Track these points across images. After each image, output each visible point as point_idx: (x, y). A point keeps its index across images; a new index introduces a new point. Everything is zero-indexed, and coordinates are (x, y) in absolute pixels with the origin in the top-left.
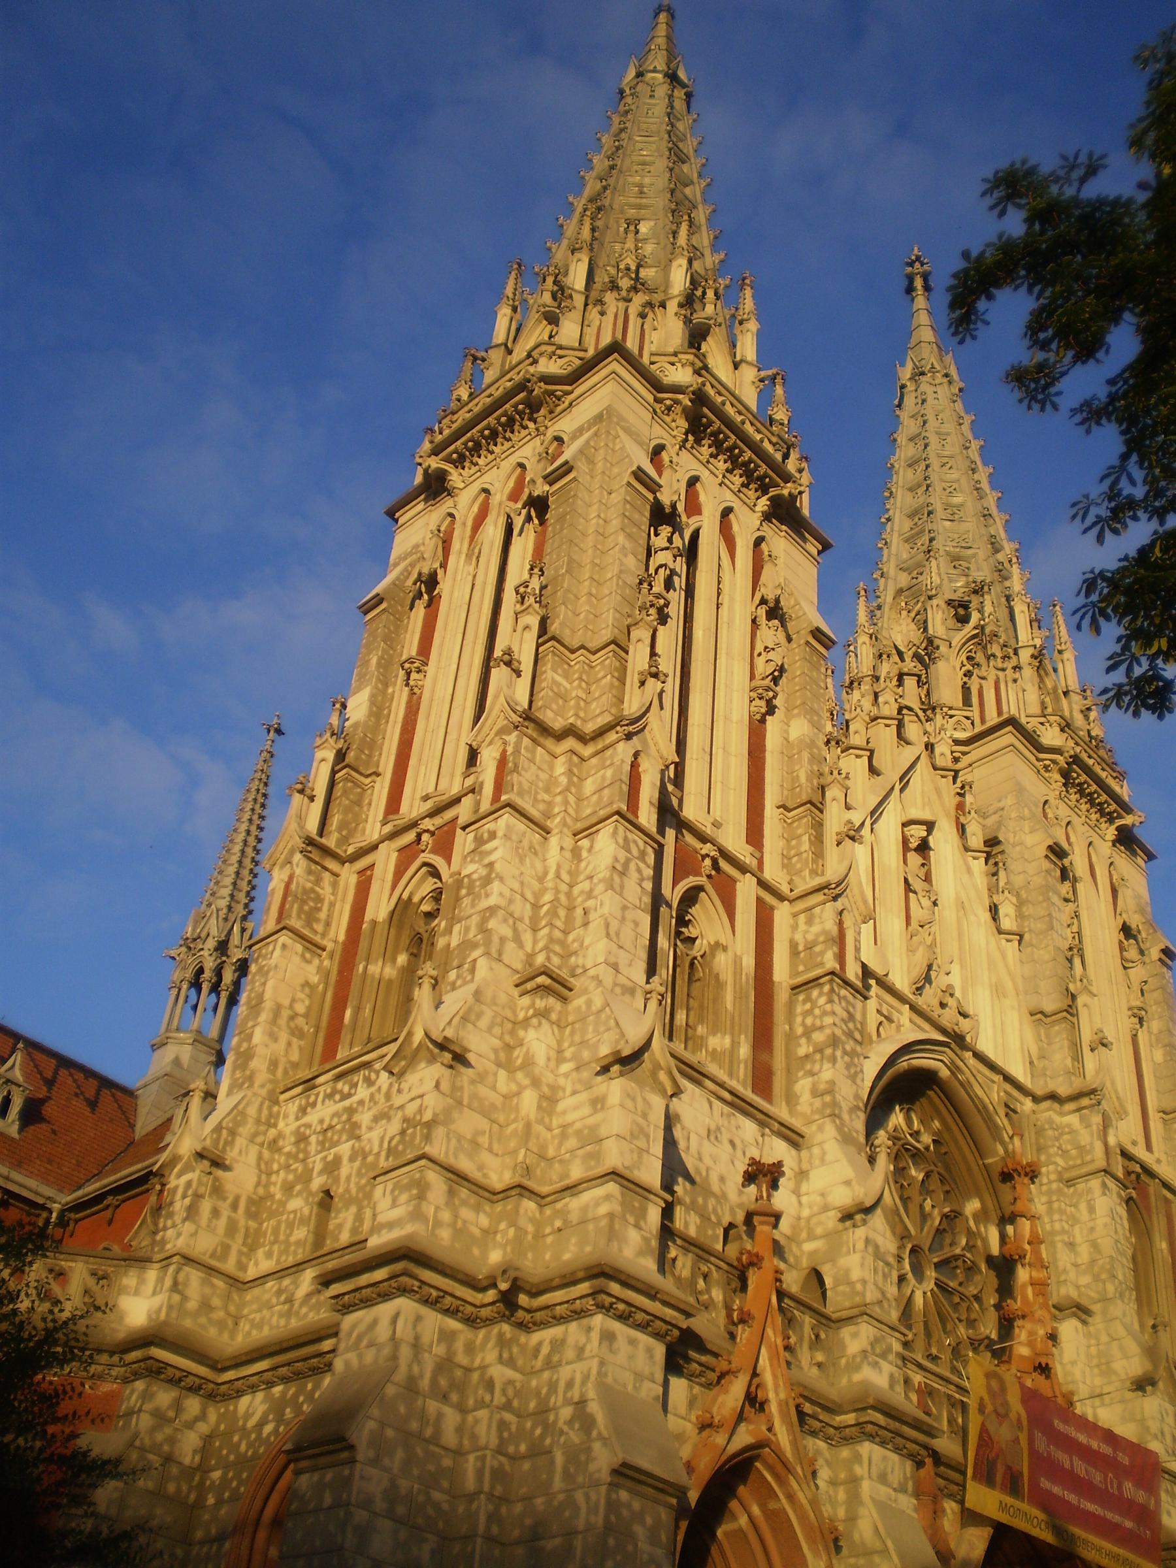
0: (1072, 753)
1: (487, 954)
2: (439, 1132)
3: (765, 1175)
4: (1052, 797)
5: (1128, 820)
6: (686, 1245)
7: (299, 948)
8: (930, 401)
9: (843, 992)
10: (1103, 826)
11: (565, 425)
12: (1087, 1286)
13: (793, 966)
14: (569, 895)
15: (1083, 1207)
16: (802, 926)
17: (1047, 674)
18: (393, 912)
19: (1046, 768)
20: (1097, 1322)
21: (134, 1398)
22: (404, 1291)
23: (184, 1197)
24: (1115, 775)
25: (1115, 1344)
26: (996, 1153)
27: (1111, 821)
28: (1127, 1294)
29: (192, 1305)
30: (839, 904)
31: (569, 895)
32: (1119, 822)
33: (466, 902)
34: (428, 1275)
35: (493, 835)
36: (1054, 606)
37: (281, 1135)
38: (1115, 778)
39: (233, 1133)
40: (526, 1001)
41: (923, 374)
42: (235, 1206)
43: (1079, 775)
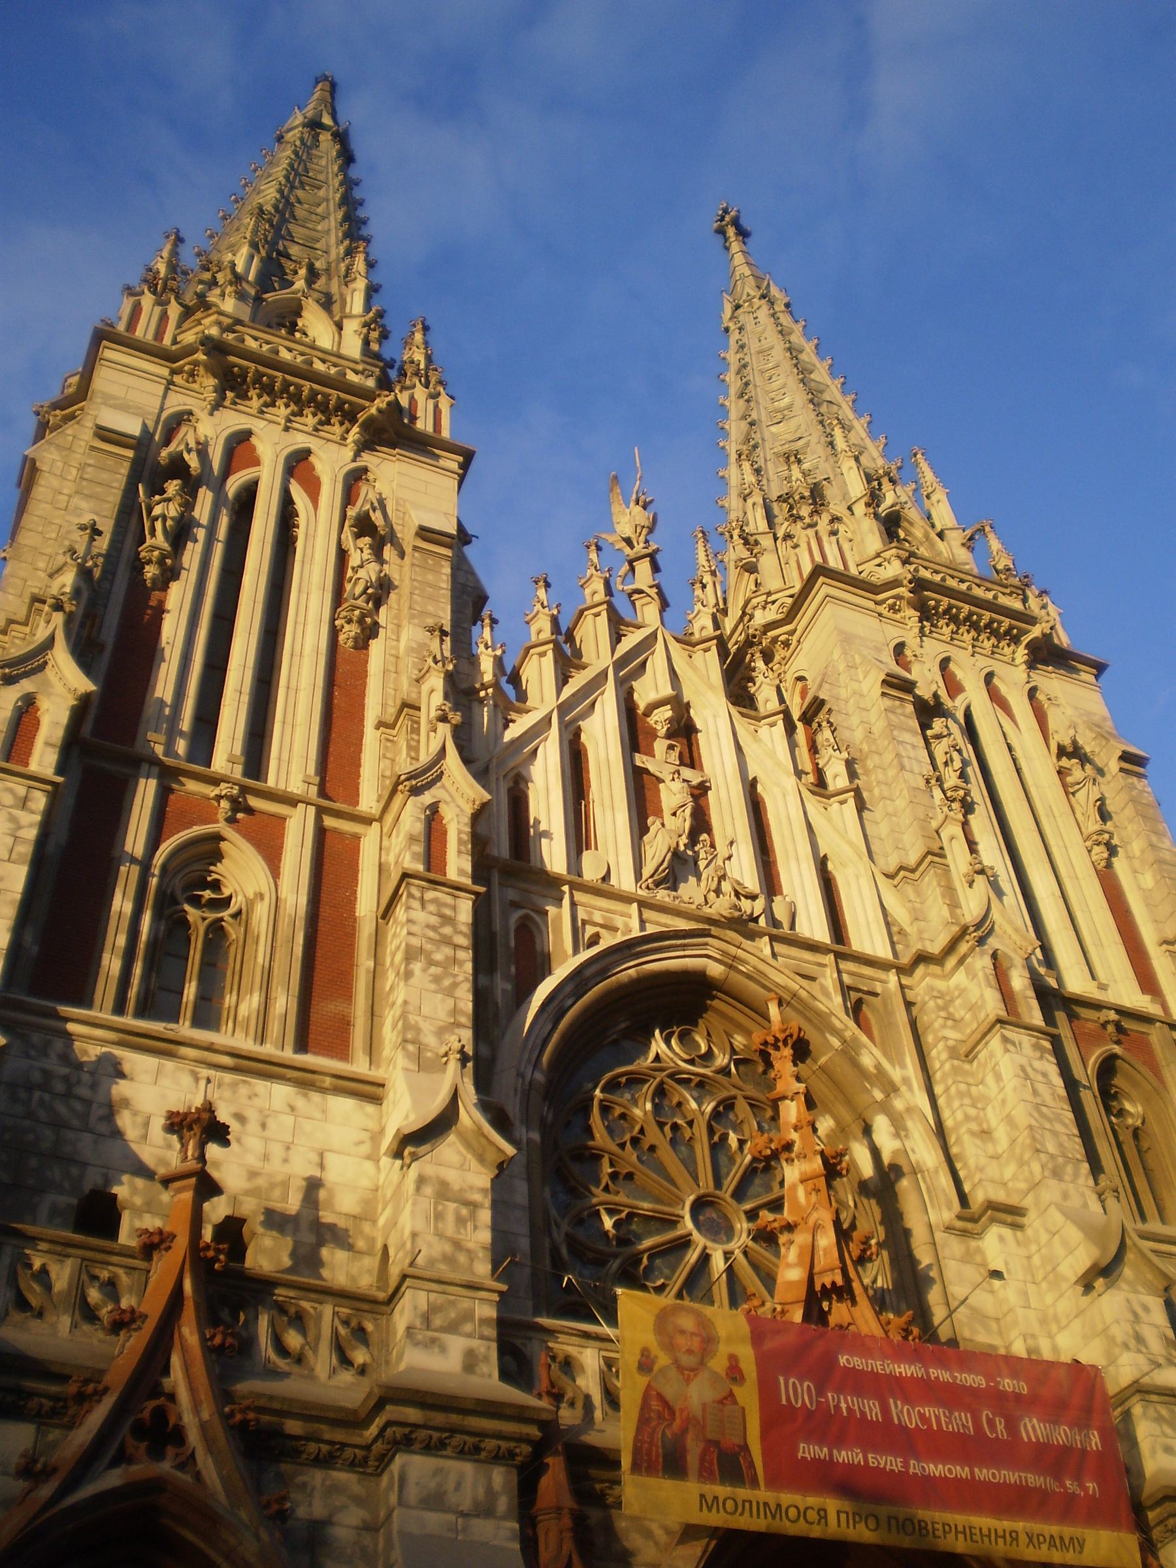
0: (909, 576)
3: (190, 1128)
4: (911, 638)
5: (1036, 632)
6: (59, 1248)
8: (750, 326)
9: (430, 895)
10: (1007, 651)
12: (1014, 1178)
15: (990, 1079)
17: (911, 524)
19: (892, 608)
20: (1032, 1220)
24: (1008, 591)
25: (1056, 1238)
26: (831, 1047)
27: (1016, 640)
28: (1069, 1169)
30: (427, 798)
32: (1026, 639)
36: (915, 455)
38: (1010, 594)
43: (938, 602)
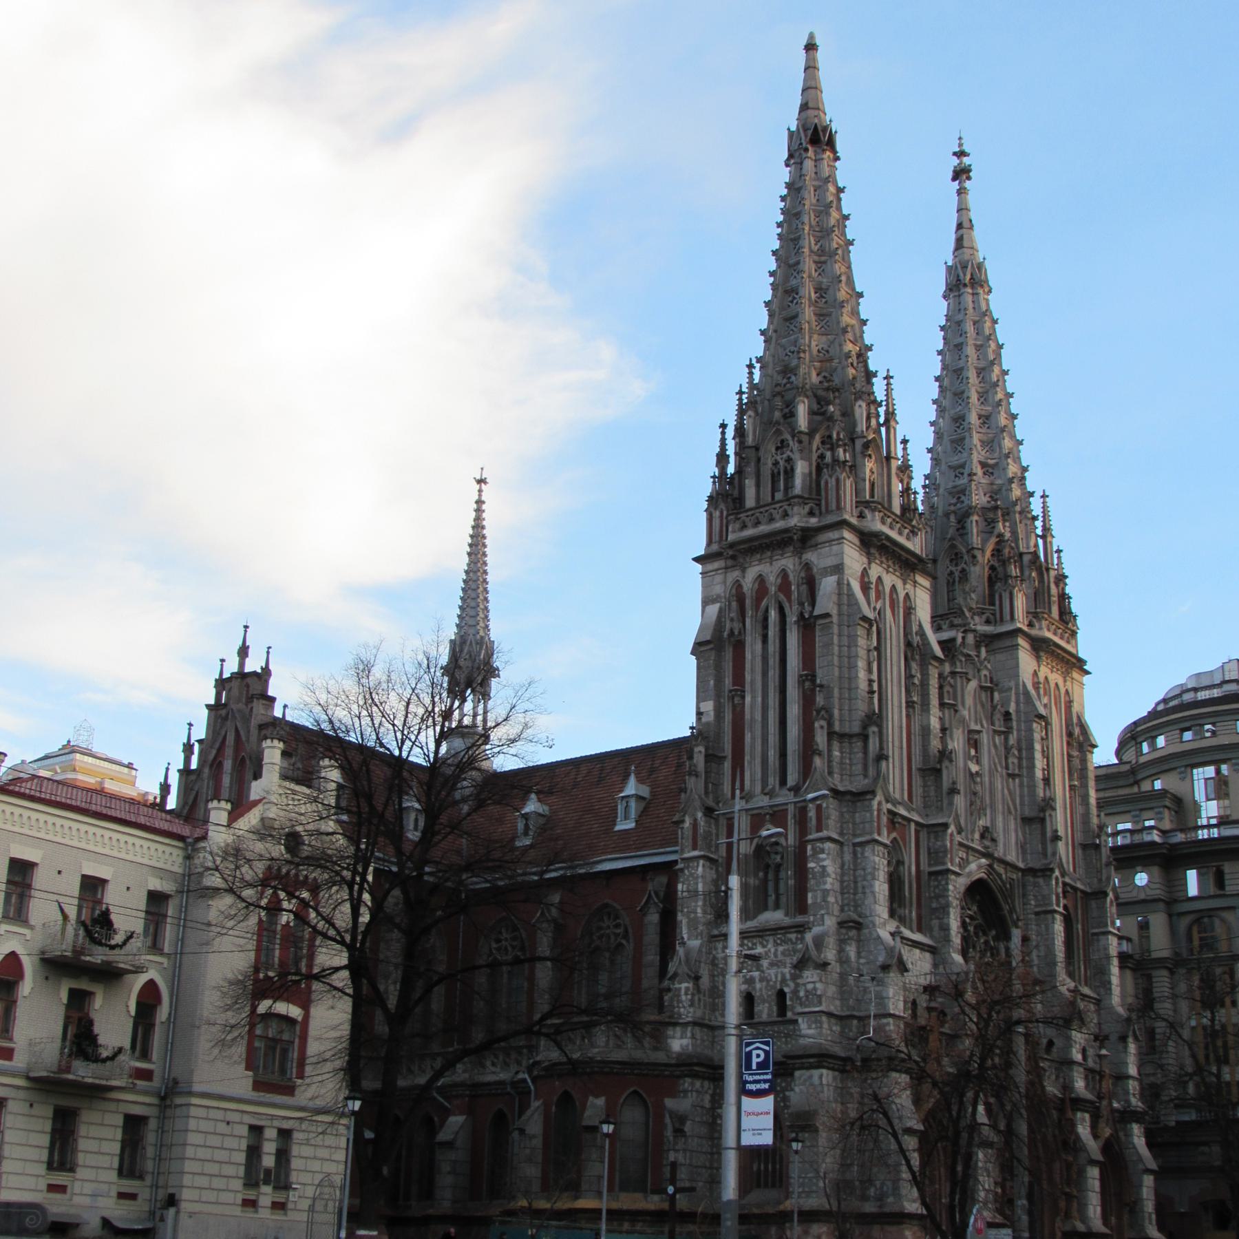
1: (828, 913)
2: (824, 999)
7: (708, 864)
11: (811, 556)
13: (929, 861)
14: (855, 877)
16: (932, 840)
18: (754, 851)
21: (686, 1085)
22: (823, 1067)
23: (686, 994)
29: (699, 1042)
31: (855, 877)
33: (812, 882)
34: (830, 1061)
35: (822, 851)
37: (715, 958)
39: (700, 962)
40: (844, 931)
41: (965, 285)
42: (704, 996)
